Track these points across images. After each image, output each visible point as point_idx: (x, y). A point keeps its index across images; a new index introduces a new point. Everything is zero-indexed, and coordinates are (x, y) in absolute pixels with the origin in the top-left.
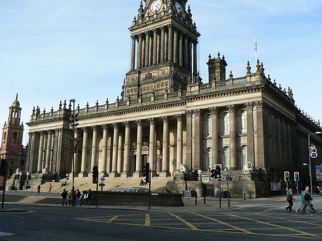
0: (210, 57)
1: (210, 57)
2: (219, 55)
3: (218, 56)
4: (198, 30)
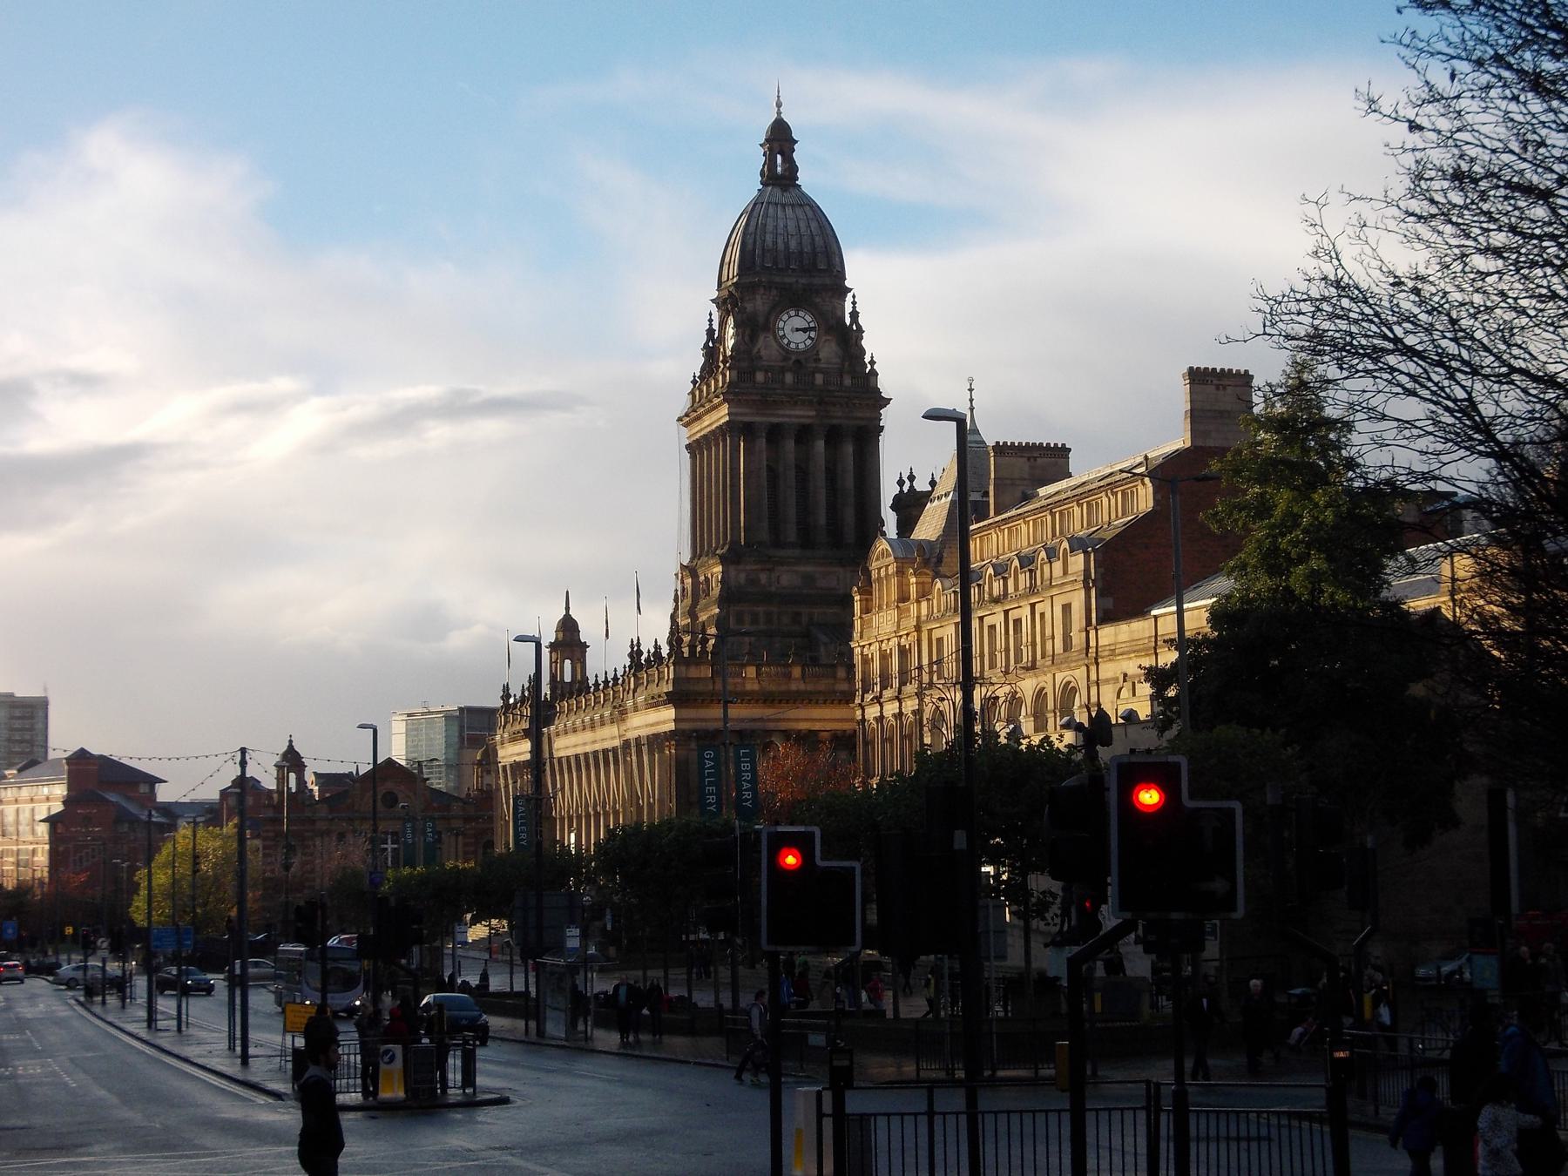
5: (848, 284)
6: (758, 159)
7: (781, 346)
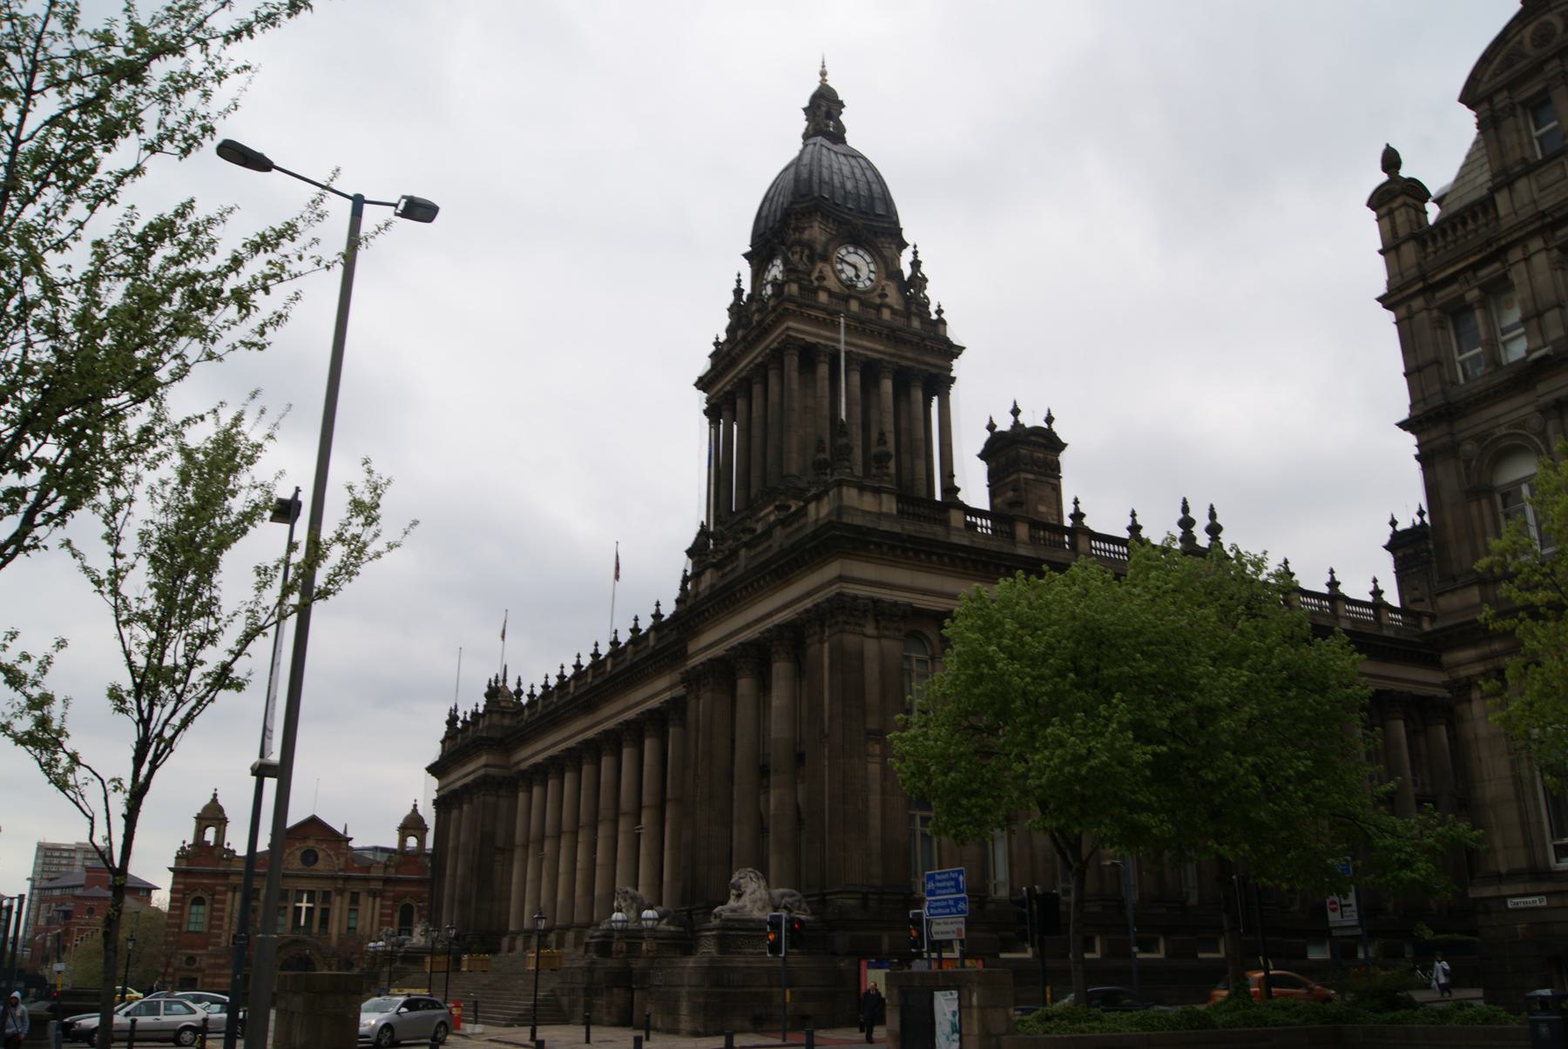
0: (991, 427)
1: (991, 427)
2: (1016, 412)
3: (1012, 418)
4: (955, 334)
5: (906, 236)
6: (802, 124)
7: (840, 280)
